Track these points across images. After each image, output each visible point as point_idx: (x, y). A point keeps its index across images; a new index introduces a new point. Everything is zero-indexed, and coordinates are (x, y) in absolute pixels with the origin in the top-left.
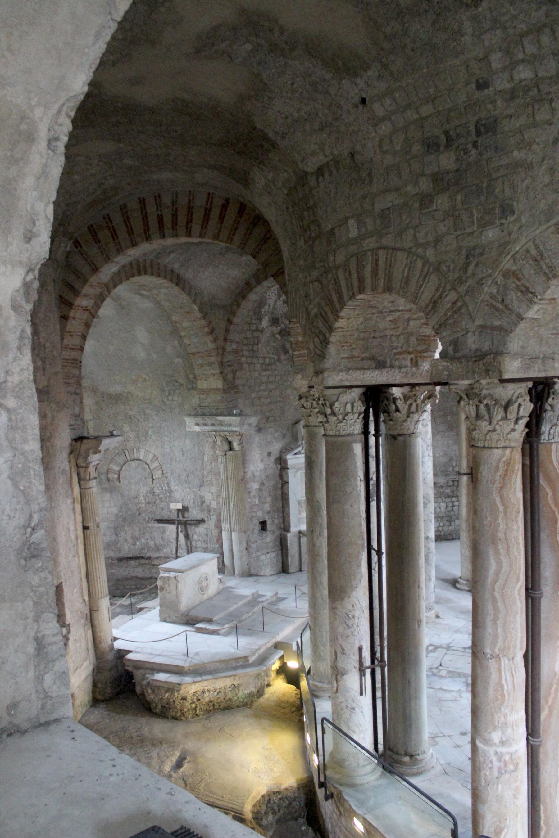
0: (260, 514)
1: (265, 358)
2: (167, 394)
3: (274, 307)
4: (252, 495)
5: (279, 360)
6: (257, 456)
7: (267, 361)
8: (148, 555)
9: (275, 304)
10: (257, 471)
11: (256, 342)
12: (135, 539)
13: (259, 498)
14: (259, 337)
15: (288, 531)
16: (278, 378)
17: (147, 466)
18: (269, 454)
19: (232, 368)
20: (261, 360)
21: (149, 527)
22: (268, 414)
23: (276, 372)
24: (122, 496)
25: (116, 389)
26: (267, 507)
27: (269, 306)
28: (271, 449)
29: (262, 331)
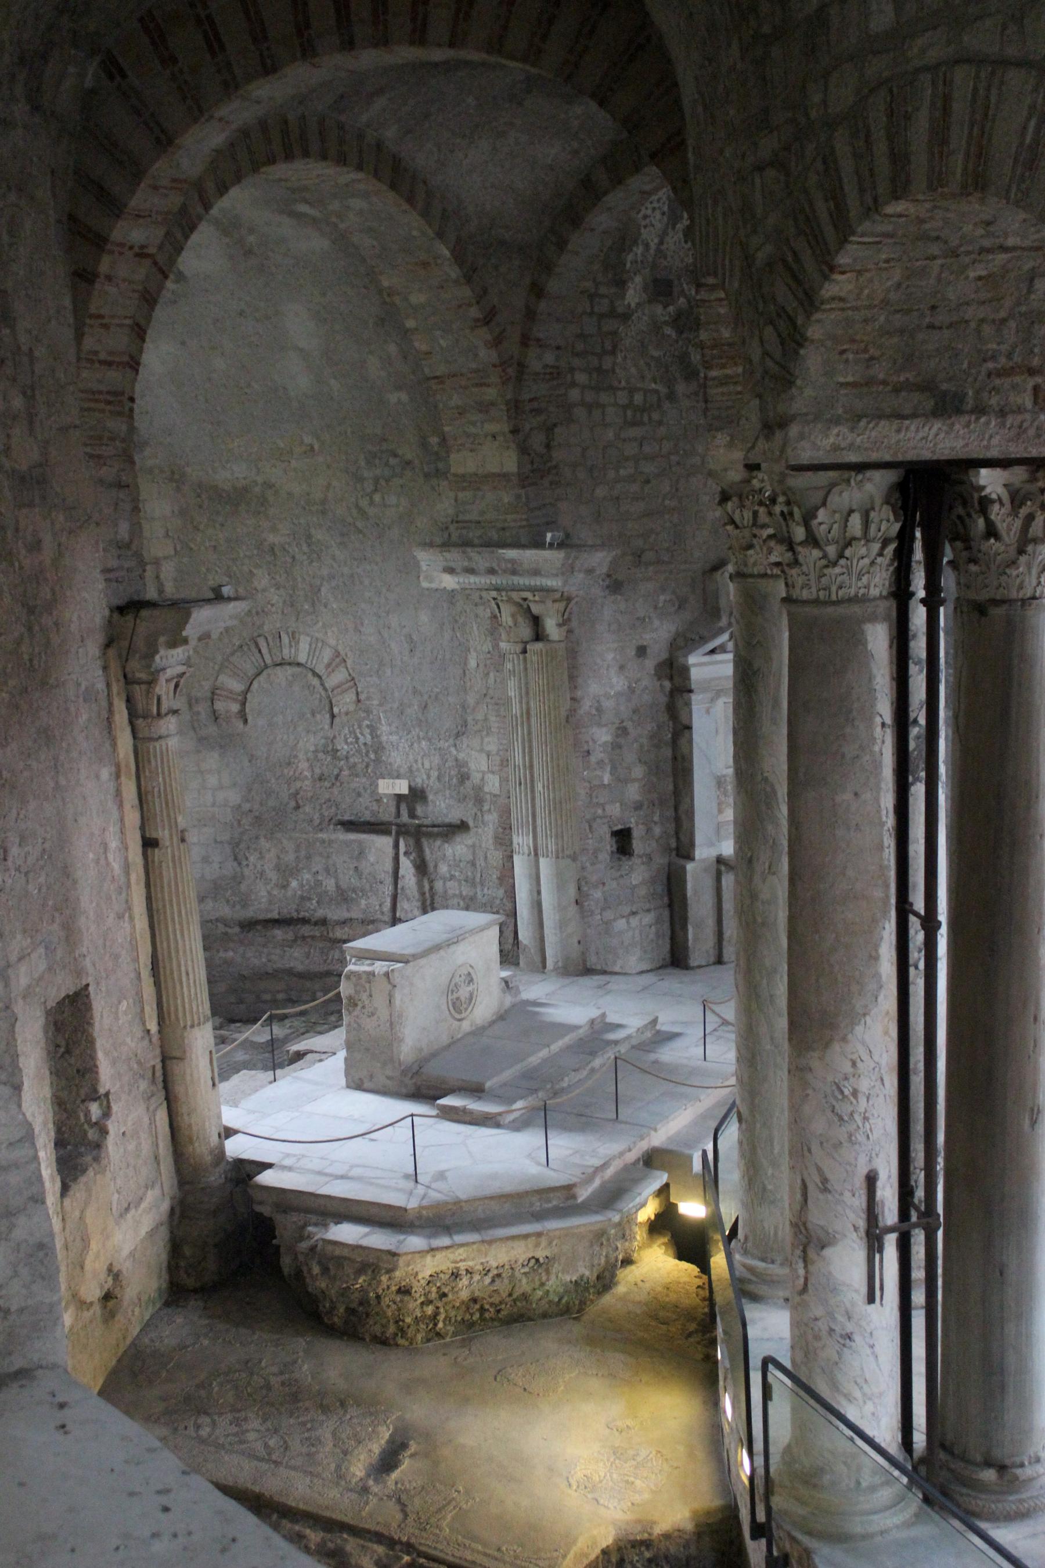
0: (614, 809)
1: (632, 391)
2: (369, 487)
3: (659, 250)
4: (593, 759)
5: (671, 396)
6: (610, 656)
7: (638, 398)
8: (320, 913)
9: (661, 242)
10: (607, 696)
11: (608, 346)
12: (286, 872)
13: (614, 769)
14: (615, 333)
15: (690, 857)
16: (667, 446)
17: (316, 682)
18: (642, 651)
19: (541, 418)
20: (622, 398)
21: (324, 841)
22: (639, 543)
23: (662, 430)
24: (252, 758)
25: (233, 473)
26: (633, 792)
27: (647, 246)
29: (626, 317)
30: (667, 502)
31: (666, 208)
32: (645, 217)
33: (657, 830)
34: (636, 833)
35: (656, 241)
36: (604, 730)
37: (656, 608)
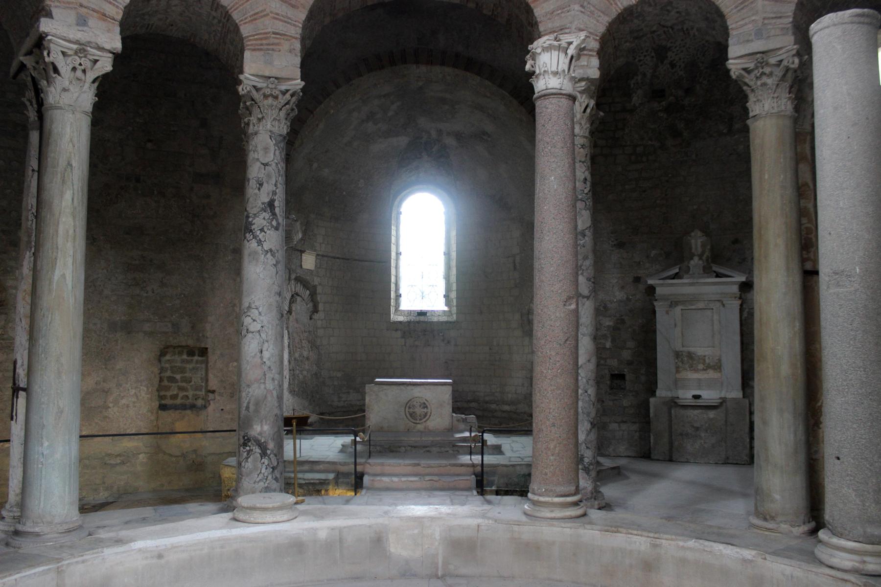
0: (614, 363)
7: (639, 150)
13: (613, 341)
15: (653, 393)
18: (637, 280)
26: (626, 355)
27: (644, 75)
30: (658, 202)
31: (653, 54)
32: (640, 61)
33: (643, 378)
34: (627, 378)
35: (651, 71)
37: (648, 257)
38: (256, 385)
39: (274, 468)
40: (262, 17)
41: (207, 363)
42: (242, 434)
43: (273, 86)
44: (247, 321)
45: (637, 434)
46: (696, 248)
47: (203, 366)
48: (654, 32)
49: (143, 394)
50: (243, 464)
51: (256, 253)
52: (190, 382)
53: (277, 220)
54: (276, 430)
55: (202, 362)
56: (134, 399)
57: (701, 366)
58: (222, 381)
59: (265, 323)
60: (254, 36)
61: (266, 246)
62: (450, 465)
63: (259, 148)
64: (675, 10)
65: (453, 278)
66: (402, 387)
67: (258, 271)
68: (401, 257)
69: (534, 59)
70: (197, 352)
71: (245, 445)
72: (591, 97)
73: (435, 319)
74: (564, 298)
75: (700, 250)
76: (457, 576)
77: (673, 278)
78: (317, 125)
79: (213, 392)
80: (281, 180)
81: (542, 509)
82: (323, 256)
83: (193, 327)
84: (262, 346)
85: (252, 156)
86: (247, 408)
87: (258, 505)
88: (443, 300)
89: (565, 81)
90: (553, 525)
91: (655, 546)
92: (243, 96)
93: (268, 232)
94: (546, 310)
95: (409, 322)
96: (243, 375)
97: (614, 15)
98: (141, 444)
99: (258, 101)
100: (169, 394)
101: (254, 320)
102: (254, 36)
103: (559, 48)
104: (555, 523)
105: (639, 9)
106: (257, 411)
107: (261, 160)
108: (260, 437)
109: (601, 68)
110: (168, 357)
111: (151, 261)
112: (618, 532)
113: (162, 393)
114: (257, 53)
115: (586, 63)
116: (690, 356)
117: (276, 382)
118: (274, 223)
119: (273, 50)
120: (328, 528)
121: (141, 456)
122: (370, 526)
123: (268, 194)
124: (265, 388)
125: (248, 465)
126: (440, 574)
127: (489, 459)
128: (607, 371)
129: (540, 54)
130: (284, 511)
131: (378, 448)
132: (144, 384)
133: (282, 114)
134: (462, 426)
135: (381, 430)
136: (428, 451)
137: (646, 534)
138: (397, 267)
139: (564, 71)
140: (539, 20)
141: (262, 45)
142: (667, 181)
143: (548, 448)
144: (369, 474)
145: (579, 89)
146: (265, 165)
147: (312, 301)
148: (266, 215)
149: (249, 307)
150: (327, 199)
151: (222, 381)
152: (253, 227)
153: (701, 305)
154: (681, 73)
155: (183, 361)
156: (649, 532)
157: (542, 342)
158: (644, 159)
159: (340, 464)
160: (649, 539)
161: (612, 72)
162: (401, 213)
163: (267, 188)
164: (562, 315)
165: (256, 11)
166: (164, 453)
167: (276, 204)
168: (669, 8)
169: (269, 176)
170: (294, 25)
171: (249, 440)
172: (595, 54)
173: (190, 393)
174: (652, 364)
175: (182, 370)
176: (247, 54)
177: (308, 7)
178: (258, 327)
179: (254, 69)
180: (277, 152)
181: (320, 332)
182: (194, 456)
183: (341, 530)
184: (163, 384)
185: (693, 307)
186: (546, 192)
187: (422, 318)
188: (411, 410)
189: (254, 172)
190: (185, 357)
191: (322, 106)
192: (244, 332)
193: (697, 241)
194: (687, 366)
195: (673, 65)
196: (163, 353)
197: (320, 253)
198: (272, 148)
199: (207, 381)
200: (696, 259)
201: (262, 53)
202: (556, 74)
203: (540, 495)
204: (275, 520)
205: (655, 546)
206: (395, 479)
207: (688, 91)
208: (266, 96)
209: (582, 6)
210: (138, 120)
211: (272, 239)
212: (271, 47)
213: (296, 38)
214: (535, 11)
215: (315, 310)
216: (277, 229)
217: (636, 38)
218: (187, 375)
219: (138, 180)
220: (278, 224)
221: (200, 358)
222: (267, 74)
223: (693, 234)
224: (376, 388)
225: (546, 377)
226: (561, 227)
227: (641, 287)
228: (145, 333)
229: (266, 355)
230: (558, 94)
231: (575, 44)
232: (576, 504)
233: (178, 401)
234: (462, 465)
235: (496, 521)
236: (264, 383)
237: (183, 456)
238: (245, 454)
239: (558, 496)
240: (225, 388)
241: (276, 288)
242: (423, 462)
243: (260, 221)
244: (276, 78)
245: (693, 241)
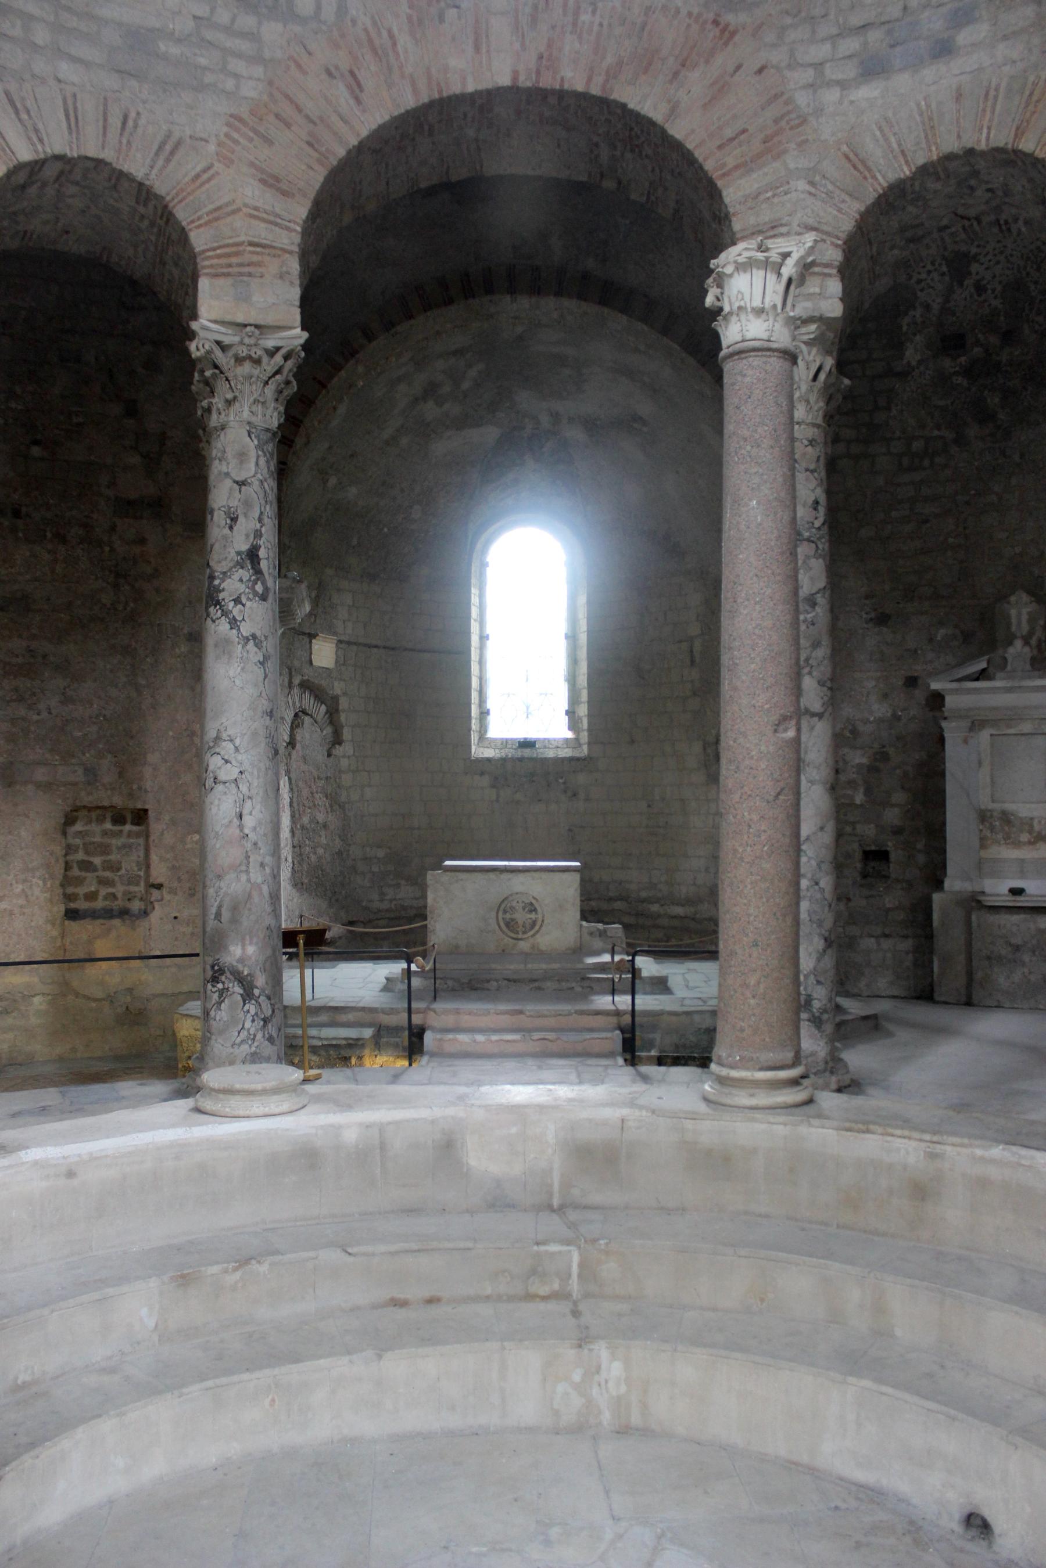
0: (869, 830)
6: (871, 684)
10: (866, 722)
13: (868, 792)
15: (937, 883)
18: (912, 682)
26: (892, 816)
27: (927, 307)
28: (918, 669)
29: (904, 375)
30: (951, 540)
31: (944, 269)
32: (919, 281)
33: (921, 859)
34: (893, 856)
35: (939, 300)
36: (859, 752)
37: (931, 640)
38: (233, 875)
39: (266, 1021)
40: (228, 214)
41: (147, 837)
42: (210, 960)
43: (252, 341)
44: (214, 762)
45: (910, 957)
46: (1019, 623)
47: (141, 841)
48: (946, 227)
49: (37, 891)
50: (212, 1013)
51: (228, 641)
52: (119, 869)
53: (264, 583)
54: (269, 952)
55: (138, 835)
56: (21, 901)
57: (1025, 837)
58: (174, 867)
59: (246, 766)
60: (214, 249)
61: (246, 629)
62: (576, 1012)
63: (229, 455)
64: (984, 187)
65: (583, 680)
66: (492, 875)
67: (231, 673)
68: (489, 644)
69: (720, 286)
70: (129, 819)
71: (215, 980)
72: (828, 352)
73: (551, 754)
74: (775, 718)
75: (1025, 628)
76: (585, 1207)
77: (977, 679)
78: (335, 408)
79: (159, 887)
80: (270, 510)
81: (735, 1091)
82: (349, 643)
83: (121, 774)
84: (242, 806)
85: (217, 468)
86: (218, 915)
87: (238, 1086)
88: (565, 720)
89: (777, 326)
90: (753, 1120)
91: (932, 1156)
92: (199, 359)
93: (248, 604)
94: (741, 740)
95: (504, 760)
96: (210, 858)
97: (870, 195)
98: (36, 980)
99: (225, 368)
100: (81, 891)
101: (227, 762)
102: (214, 249)
103: (766, 264)
104: (758, 1115)
105: (917, 187)
106: (234, 921)
107: (233, 475)
108: (240, 967)
109: (846, 297)
110: (78, 827)
111: (44, 656)
112: (868, 1131)
113: (70, 890)
114: (221, 281)
115: (817, 290)
116: (1006, 818)
117: (268, 870)
118: (259, 588)
119: (250, 275)
120: (360, 1124)
121: (37, 1000)
122: (433, 1122)
123: (247, 536)
124: (248, 880)
125: (222, 1015)
126: (556, 1203)
127: (645, 1002)
128: (856, 846)
129: (731, 276)
130: (284, 1096)
131: (450, 983)
132: (38, 874)
133: (270, 391)
134: (598, 943)
135: (454, 951)
136: (539, 988)
137: (916, 1135)
138: (481, 662)
139: (775, 306)
140: (731, 210)
141: (230, 266)
142: (967, 503)
143: (745, 985)
144: (433, 1029)
145: (805, 338)
146: (241, 484)
147: (331, 723)
148: (245, 574)
149: (218, 739)
150: (355, 542)
151: (174, 867)
152: (221, 596)
153: (1027, 727)
154: (996, 303)
155: (105, 833)
156: (923, 1131)
157: (736, 797)
158: (926, 463)
159: (384, 1011)
160: (923, 1145)
161: (867, 305)
162: (487, 565)
163: (246, 525)
164: (771, 749)
165: (218, 204)
166: (77, 995)
167: (262, 553)
168: (973, 182)
169: (247, 504)
170: (288, 229)
171: (222, 971)
172: (834, 271)
173: (119, 890)
174: (935, 833)
175: (105, 850)
176: (204, 284)
177: (312, 195)
178: (234, 773)
179: (216, 311)
180: (262, 461)
181: (347, 779)
182: (129, 999)
183: (382, 1128)
184: (70, 874)
185: (1012, 731)
186: (743, 527)
187: (527, 753)
188: (508, 916)
189: (222, 496)
190: (108, 825)
191: (343, 373)
192: (209, 783)
193: (1020, 611)
194: (1000, 836)
195: (980, 288)
196: (69, 820)
197: (343, 638)
198: (253, 453)
199: (148, 867)
200: (1018, 643)
201: (229, 281)
202: (759, 312)
203: (732, 1067)
204: (267, 1110)
205: (932, 1156)
206: (480, 1038)
207: (1009, 336)
208: (239, 360)
209: (812, 183)
210: (13, 405)
211: (256, 616)
212: (246, 270)
213: (291, 252)
214: (724, 194)
215: (337, 740)
216: (264, 598)
217: (911, 240)
218: (113, 857)
219: (17, 514)
220: (266, 589)
221: (135, 828)
222: (240, 319)
223: (1013, 599)
224: (446, 877)
225: (742, 859)
226: (769, 591)
227: (919, 695)
228: (39, 785)
229: (249, 822)
230: (764, 350)
231: (795, 256)
232: (795, 1082)
233: (99, 904)
234: (598, 1013)
235: (653, 1112)
236: (247, 872)
237: (111, 999)
238: (216, 996)
239: (761, 1069)
240: (179, 880)
241: (264, 704)
242: (530, 1007)
243: (233, 584)
244: (257, 326)
245: (1013, 612)
